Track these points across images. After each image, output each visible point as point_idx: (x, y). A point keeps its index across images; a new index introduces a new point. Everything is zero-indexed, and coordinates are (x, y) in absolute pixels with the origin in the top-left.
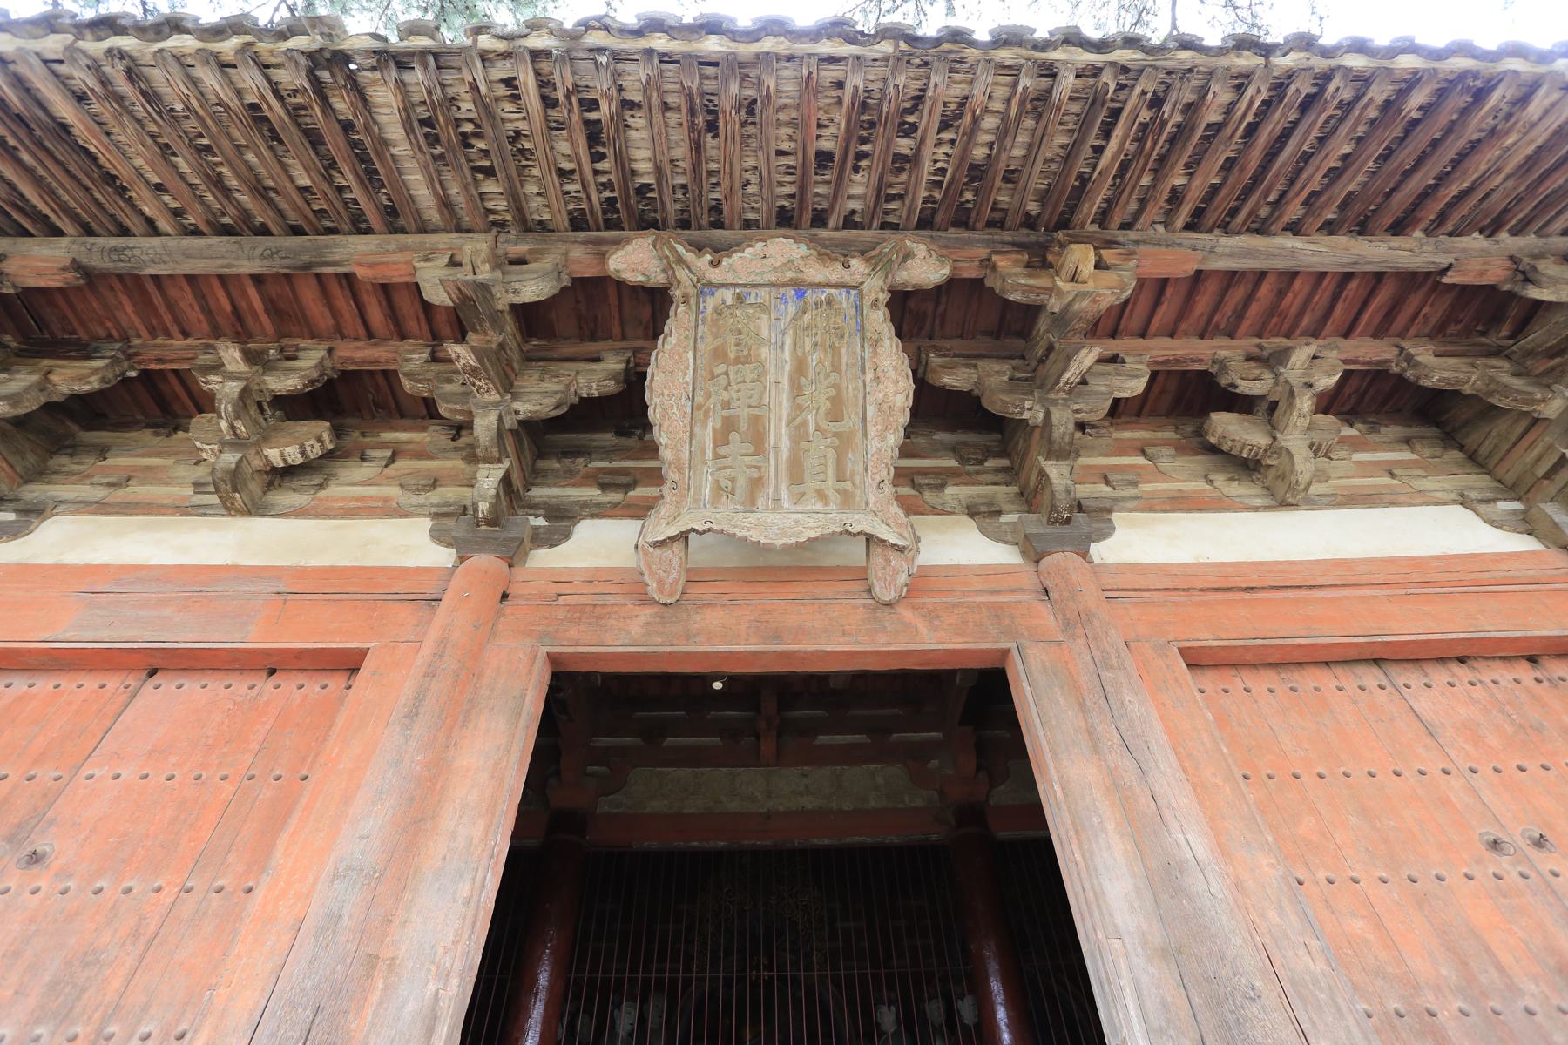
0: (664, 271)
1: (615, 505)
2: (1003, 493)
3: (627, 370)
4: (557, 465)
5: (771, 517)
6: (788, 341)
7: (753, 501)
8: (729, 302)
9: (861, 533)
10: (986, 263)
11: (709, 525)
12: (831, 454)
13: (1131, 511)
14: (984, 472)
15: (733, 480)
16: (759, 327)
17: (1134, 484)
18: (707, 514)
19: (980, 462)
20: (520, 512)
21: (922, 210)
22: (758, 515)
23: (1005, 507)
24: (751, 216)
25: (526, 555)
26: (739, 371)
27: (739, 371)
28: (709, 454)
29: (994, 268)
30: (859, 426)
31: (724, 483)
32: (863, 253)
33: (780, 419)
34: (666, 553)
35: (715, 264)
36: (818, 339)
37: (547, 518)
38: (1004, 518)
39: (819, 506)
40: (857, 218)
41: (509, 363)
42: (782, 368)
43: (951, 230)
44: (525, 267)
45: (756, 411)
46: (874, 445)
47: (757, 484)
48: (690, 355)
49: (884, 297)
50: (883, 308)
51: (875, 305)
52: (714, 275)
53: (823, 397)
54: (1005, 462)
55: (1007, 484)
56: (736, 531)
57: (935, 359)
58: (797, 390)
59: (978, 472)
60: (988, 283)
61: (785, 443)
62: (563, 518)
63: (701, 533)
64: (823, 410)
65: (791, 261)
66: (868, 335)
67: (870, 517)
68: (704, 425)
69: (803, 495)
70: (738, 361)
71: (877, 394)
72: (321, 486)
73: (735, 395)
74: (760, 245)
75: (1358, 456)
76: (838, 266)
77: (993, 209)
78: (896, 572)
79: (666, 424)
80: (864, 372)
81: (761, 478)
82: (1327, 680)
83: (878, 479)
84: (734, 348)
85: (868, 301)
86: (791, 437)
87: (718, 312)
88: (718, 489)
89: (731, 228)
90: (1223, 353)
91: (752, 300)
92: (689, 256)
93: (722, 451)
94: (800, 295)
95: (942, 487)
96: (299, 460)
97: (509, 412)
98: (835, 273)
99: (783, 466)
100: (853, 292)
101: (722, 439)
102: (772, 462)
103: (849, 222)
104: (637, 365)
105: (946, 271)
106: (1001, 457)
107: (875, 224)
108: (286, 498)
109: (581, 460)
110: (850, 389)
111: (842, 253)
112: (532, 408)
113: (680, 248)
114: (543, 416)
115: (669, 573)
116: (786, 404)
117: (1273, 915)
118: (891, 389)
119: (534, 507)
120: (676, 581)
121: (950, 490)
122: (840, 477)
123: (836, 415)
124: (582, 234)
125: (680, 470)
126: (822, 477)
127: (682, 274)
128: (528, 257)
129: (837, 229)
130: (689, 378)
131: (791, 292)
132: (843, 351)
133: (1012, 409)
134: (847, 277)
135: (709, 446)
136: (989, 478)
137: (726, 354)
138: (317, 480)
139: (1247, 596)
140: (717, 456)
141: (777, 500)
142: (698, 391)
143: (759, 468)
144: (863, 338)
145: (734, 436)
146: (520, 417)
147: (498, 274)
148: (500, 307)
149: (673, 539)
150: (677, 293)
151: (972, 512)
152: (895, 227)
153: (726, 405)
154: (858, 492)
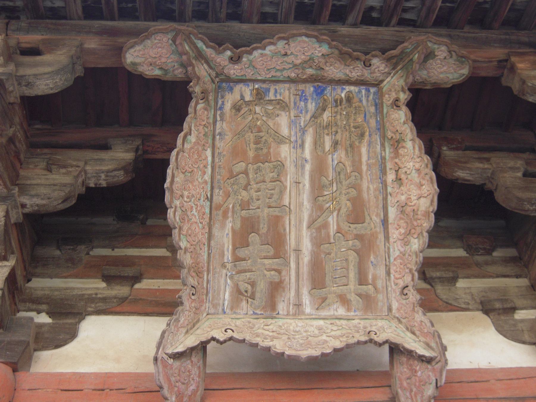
0: (183, 66)
1: (123, 300)
2: (515, 284)
3: (136, 160)
4: (58, 253)
5: (294, 324)
7: (271, 306)
8: (248, 98)
9: (386, 342)
10: (504, 64)
11: (230, 333)
12: (353, 256)
14: (494, 263)
15: (253, 284)
16: (279, 125)
18: (226, 320)
19: (489, 252)
20: (21, 306)
21: (441, 8)
22: (280, 322)
23: (518, 302)
24: (268, 9)
25: (30, 359)
26: (259, 169)
27: (259, 169)
28: (228, 256)
29: (513, 69)
30: (379, 229)
31: (243, 286)
32: (384, 51)
33: (301, 222)
34: (187, 364)
35: (235, 60)
36: (338, 137)
37: (50, 314)
38: (520, 315)
39: (341, 311)
40: (375, 15)
41: (17, 155)
42: (303, 167)
43: (467, 28)
44: (38, 58)
45: (276, 212)
46: (396, 249)
47: (276, 288)
48: (209, 153)
49: (404, 97)
50: (404, 109)
51: (396, 104)
52: (234, 71)
53: (344, 198)
54: (512, 252)
55: (517, 276)
56: (258, 340)
57: (448, 153)
58: (318, 189)
59: (487, 263)
60: (504, 82)
61: (307, 246)
62: (67, 314)
63: (221, 343)
64: (344, 210)
65: (311, 59)
66: (389, 134)
67: (394, 323)
68: (223, 226)
69: (324, 299)
70: (257, 159)
71: (398, 196)
73: (254, 195)
74: (281, 44)
76: (360, 65)
77: (510, 10)
78: (424, 383)
79: (185, 228)
80: (384, 172)
81: (281, 282)
83: (401, 284)
84: (253, 146)
85: (388, 100)
86: (311, 241)
87: (237, 108)
89: (249, 21)
92: (209, 52)
93: (242, 253)
94: (320, 92)
95: (454, 280)
97: (16, 207)
98: (356, 71)
99: (305, 270)
100: (372, 90)
101: (241, 240)
102: (293, 265)
103: (368, 19)
104: (145, 152)
105: (465, 71)
106: (507, 246)
107: (394, 21)
109: (82, 248)
110: (369, 187)
111: (362, 51)
112: (39, 201)
113: (200, 44)
114: (51, 209)
115: (187, 384)
116: (307, 205)
118: (414, 192)
119: (36, 302)
120: (195, 392)
121: (461, 283)
122: (362, 280)
123: (357, 215)
124: (97, 24)
125: (199, 274)
126: (344, 280)
127: (202, 70)
128: (41, 47)
129: (354, 25)
130: (207, 177)
131: (310, 89)
132: (364, 150)
133: (527, 206)
134: (367, 74)
135: (228, 247)
136: (500, 269)
137: (245, 153)
140: (237, 259)
141: (299, 305)
142: (216, 191)
143: (279, 272)
144: (383, 137)
145: (253, 238)
146: (26, 211)
147: (11, 67)
148: (12, 100)
149: (192, 349)
150: (196, 89)
151: (487, 308)
152: (412, 24)
153: (245, 205)
154: (380, 297)
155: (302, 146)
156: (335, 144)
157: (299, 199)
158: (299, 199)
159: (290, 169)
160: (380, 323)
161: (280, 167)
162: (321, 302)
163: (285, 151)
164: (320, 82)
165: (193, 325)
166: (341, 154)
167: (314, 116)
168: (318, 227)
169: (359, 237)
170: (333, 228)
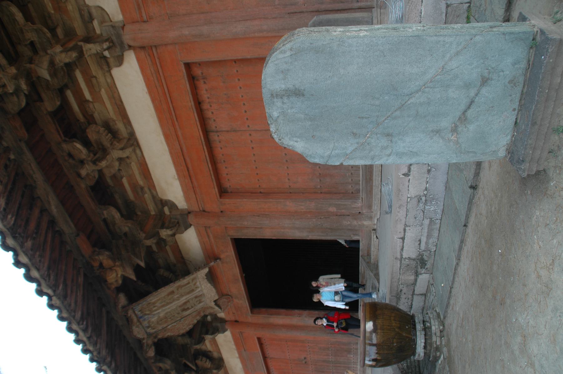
6: (155, 312)
7: (201, 295)
13: (157, 192)
17: (142, 188)
35: (144, 339)
39: (198, 283)
47: (196, 297)
48: (169, 327)
58: (168, 304)
61: (184, 298)
72: (210, 352)
75: (88, 96)
82: (219, 152)
87: (154, 329)
88: (200, 303)
90: (83, 186)
91: (147, 325)
92: (145, 345)
94: (141, 317)
96: (208, 360)
99: (190, 295)
108: (215, 355)
116: (173, 304)
117: (302, 207)
122: (189, 283)
125: (199, 313)
127: (150, 342)
130: (175, 324)
131: (141, 320)
132: (153, 301)
135: (190, 310)
138: (209, 353)
139: (192, 172)
140: (192, 307)
145: (186, 307)
150: (156, 340)
153: (178, 313)
155: (159, 313)
156: (154, 307)
157: (174, 305)
158: (174, 305)
159: (166, 311)
160: (199, 276)
161: (166, 313)
162: (197, 288)
163: (162, 315)
164: (139, 319)
165: (212, 308)
166: (156, 305)
167: (148, 314)
168: (178, 299)
169: (178, 289)
170: (178, 296)
